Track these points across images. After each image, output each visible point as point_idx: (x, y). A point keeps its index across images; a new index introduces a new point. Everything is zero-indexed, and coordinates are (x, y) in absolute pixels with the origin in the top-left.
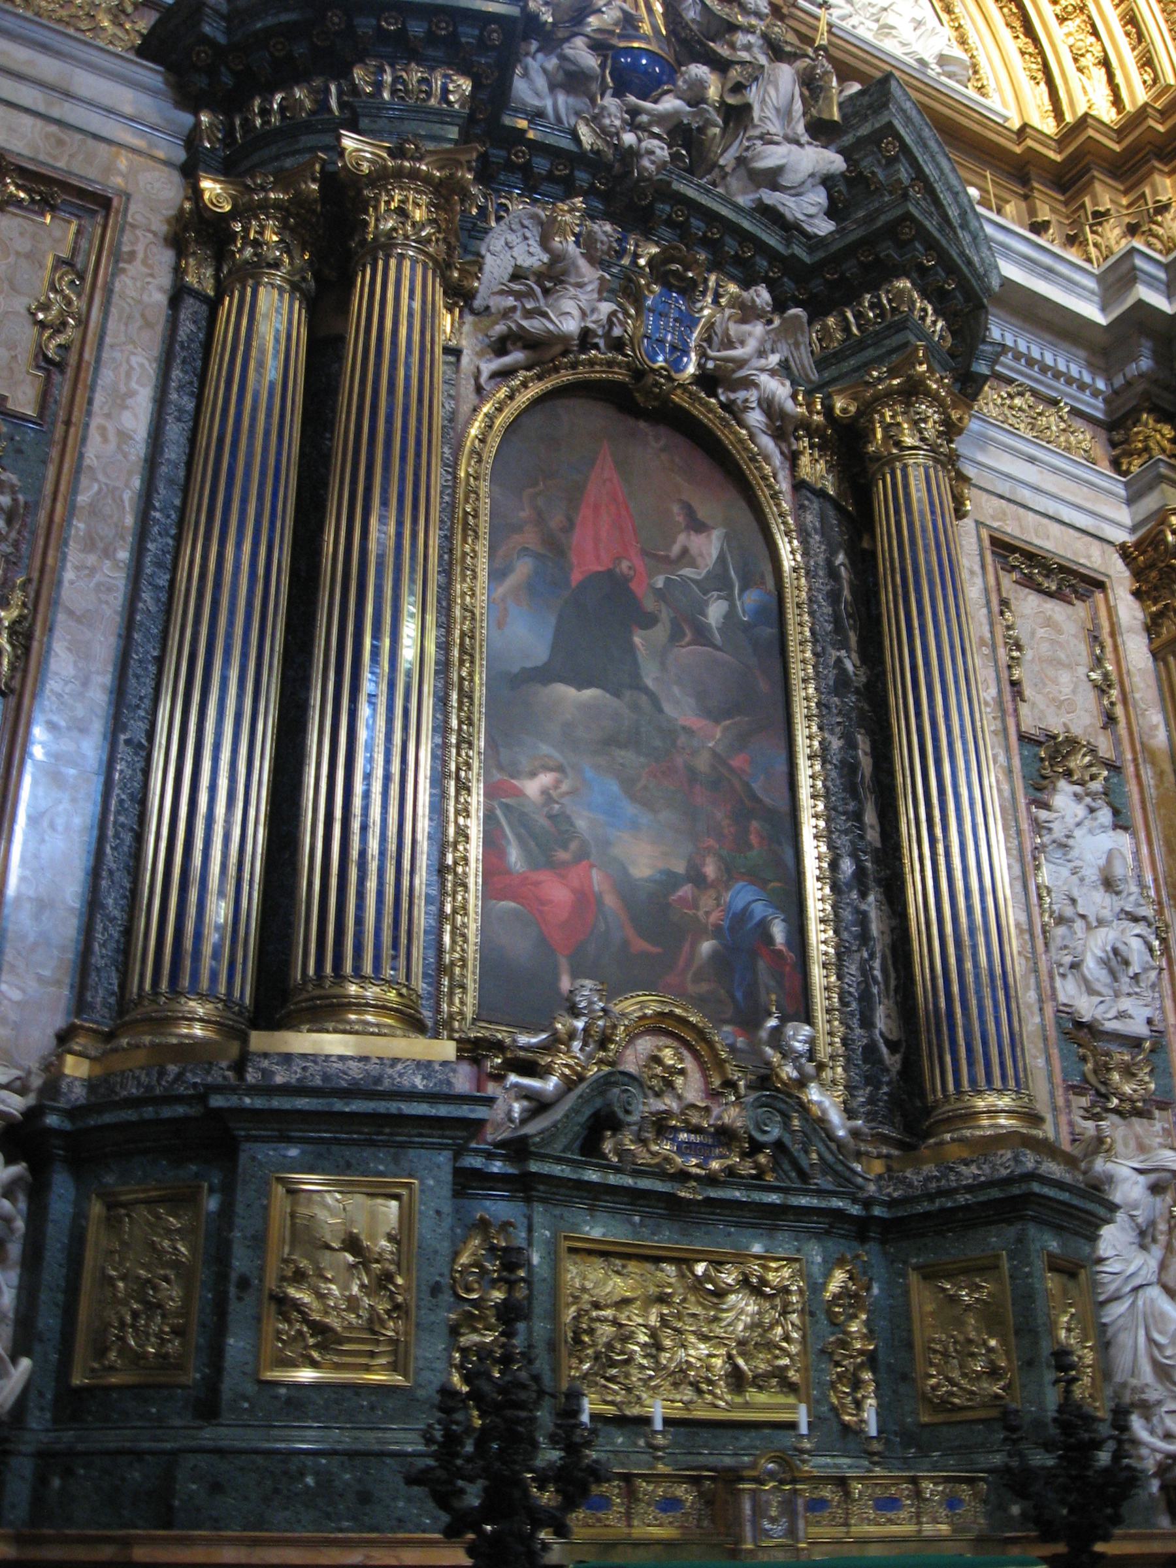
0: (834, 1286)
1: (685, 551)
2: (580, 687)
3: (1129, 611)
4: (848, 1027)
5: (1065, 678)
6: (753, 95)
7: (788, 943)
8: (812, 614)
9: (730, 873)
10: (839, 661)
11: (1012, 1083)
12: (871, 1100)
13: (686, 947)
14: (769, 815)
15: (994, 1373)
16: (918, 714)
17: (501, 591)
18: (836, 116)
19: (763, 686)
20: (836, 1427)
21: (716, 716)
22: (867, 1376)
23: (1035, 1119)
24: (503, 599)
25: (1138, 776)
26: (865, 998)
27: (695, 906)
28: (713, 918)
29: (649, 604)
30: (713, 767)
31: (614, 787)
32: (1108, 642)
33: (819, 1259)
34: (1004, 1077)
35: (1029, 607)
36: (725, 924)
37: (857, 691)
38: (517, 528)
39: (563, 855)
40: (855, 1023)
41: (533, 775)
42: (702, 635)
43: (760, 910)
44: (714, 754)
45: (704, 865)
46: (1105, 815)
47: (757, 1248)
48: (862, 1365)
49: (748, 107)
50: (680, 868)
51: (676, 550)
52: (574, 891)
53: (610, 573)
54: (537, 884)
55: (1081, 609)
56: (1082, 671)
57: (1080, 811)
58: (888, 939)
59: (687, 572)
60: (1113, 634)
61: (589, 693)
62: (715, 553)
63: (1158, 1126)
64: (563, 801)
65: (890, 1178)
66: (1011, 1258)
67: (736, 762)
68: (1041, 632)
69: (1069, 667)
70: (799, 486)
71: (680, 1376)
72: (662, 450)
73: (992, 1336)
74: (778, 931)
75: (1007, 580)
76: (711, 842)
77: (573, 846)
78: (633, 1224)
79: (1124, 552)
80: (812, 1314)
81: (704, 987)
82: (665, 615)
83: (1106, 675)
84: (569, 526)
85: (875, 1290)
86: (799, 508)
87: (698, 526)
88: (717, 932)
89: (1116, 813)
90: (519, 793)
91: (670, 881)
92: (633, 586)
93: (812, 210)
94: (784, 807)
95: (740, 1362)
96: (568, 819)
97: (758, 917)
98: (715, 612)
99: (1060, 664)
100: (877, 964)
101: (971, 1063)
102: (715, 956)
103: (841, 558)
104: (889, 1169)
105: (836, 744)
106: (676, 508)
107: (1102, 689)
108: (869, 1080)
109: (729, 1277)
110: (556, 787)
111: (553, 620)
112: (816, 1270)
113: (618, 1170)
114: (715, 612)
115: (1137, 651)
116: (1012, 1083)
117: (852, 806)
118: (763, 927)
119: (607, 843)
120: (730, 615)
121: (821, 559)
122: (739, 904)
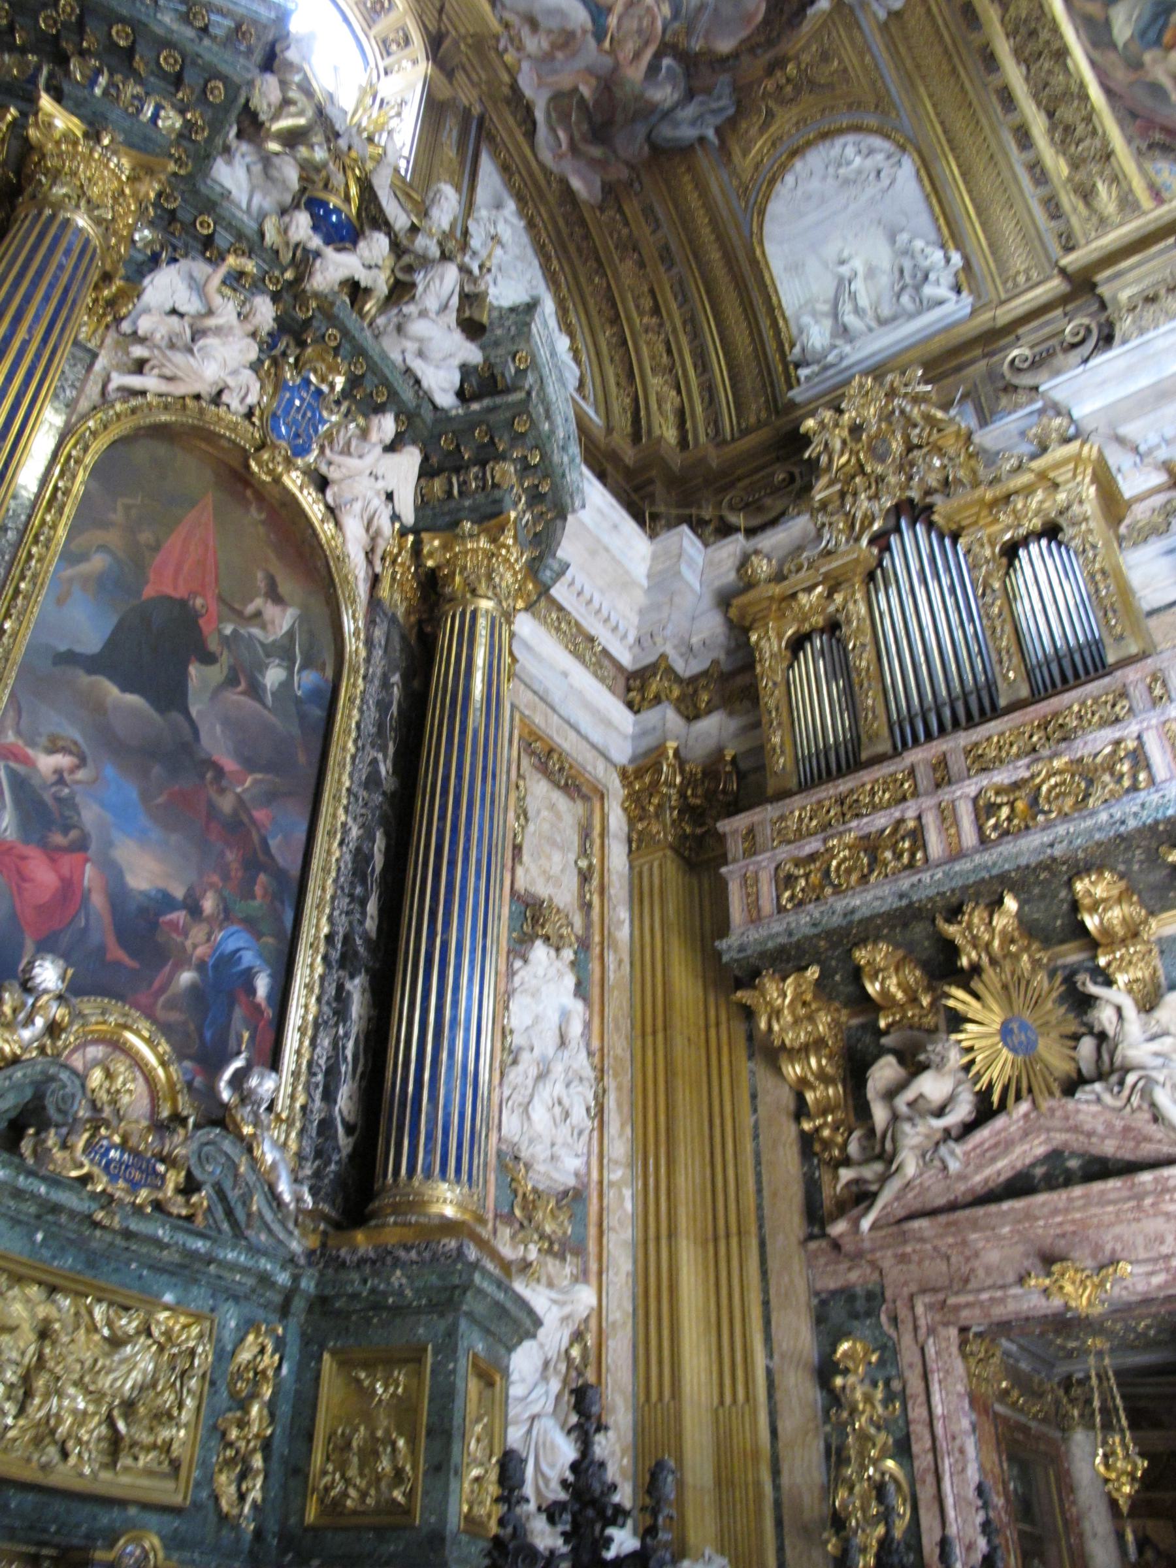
0: (245, 1356)
1: (258, 614)
2: (124, 689)
3: (617, 820)
4: (310, 1096)
5: (557, 857)
6: (419, 278)
7: (269, 997)
8: (361, 711)
9: (226, 914)
10: (374, 762)
11: (465, 1177)
12: (317, 1174)
13: (167, 968)
14: (279, 875)
15: (399, 1476)
16: (442, 818)
17: (70, 572)
18: (485, 319)
19: (302, 758)
20: (212, 1518)
21: (250, 764)
22: (257, 1462)
23: (481, 1220)
24: (71, 580)
25: (602, 957)
26: (332, 1072)
27: (186, 934)
28: (199, 951)
29: (213, 645)
30: (235, 813)
31: (134, 795)
32: (598, 841)
33: (233, 1324)
34: (458, 1170)
35: (539, 790)
36: (211, 962)
37: (384, 793)
38: (105, 525)
39: (58, 839)
40: (318, 1095)
41: (52, 750)
42: (255, 690)
43: (248, 958)
44: (239, 797)
45: (203, 896)
46: (570, 981)
47: (168, 1298)
48: (254, 1450)
49: (413, 285)
50: (179, 893)
51: (250, 609)
52: (62, 879)
53: (183, 603)
54: (23, 858)
55: (580, 808)
56: (572, 857)
57: (552, 972)
58: (364, 1023)
59: (256, 631)
60: (602, 836)
61: (133, 699)
62: (285, 628)
63: (568, 1270)
64: (76, 787)
65: (322, 1255)
66: (436, 1353)
67: (259, 814)
68: (545, 813)
69: (562, 848)
70: (374, 602)
71: (45, 1432)
72: (263, 522)
73: (401, 1434)
74: (262, 985)
75: (525, 762)
76: (215, 879)
77: (74, 834)
78: (33, 1242)
79: (624, 774)
80: (213, 1383)
81: (174, 1017)
82: (225, 659)
83: (590, 866)
84: (156, 548)
85: (285, 1371)
86: (371, 622)
87: (276, 598)
88: (201, 967)
89: (579, 984)
90: (27, 761)
91: (166, 902)
92: (201, 622)
93: (446, 385)
94: (295, 871)
95: (121, 1425)
96: (75, 808)
97: (245, 964)
98: (273, 676)
99: (554, 844)
100: (350, 1045)
101: (429, 1152)
102: (193, 988)
103: (396, 678)
104: (324, 1245)
105: (355, 832)
106: (260, 575)
107: (584, 877)
108: (319, 1153)
109: (128, 1324)
110: (72, 771)
111: (114, 620)
112: (228, 1338)
113: (30, 1173)
114: (273, 676)
115: (618, 858)
116: (465, 1177)
117: (358, 890)
118: (248, 977)
119: (110, 844)
120: (287, 685)
121: (379, 672)
122: (231, 946)
